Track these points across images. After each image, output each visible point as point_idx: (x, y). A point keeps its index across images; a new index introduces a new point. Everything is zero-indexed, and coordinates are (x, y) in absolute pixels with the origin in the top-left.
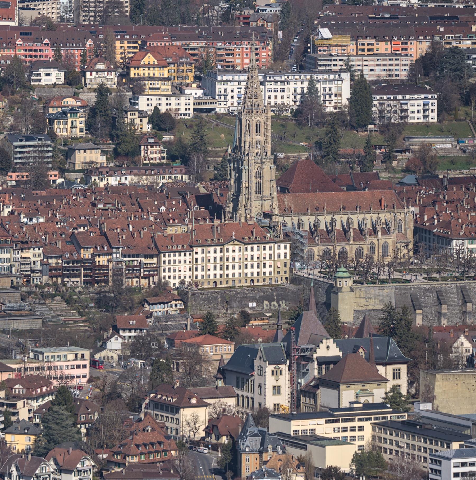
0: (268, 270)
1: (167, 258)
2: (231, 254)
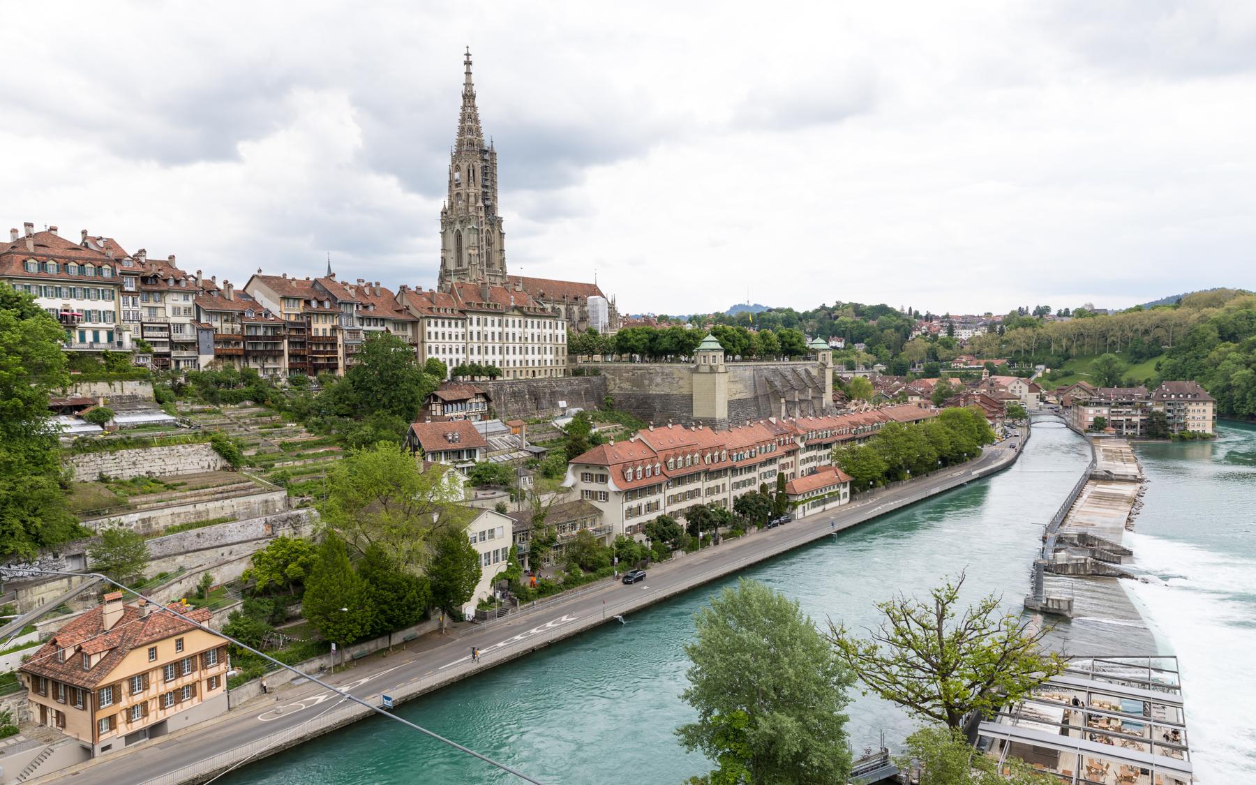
0: (549, 357)
1: (432, 329)
2: (510, 330)
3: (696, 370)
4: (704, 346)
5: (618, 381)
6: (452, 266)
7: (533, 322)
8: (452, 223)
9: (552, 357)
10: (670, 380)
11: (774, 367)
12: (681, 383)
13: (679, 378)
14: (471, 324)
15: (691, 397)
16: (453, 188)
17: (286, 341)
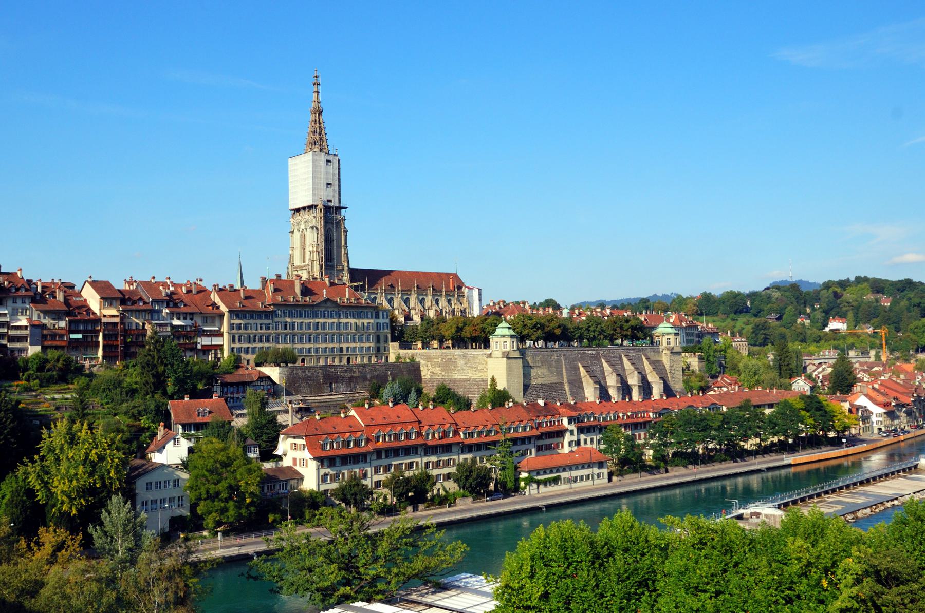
3: (490, 356)
4: (499, 331)
5: (430, 367)
9: (372, 345)
11: (594, 352)
17: (101, 334)
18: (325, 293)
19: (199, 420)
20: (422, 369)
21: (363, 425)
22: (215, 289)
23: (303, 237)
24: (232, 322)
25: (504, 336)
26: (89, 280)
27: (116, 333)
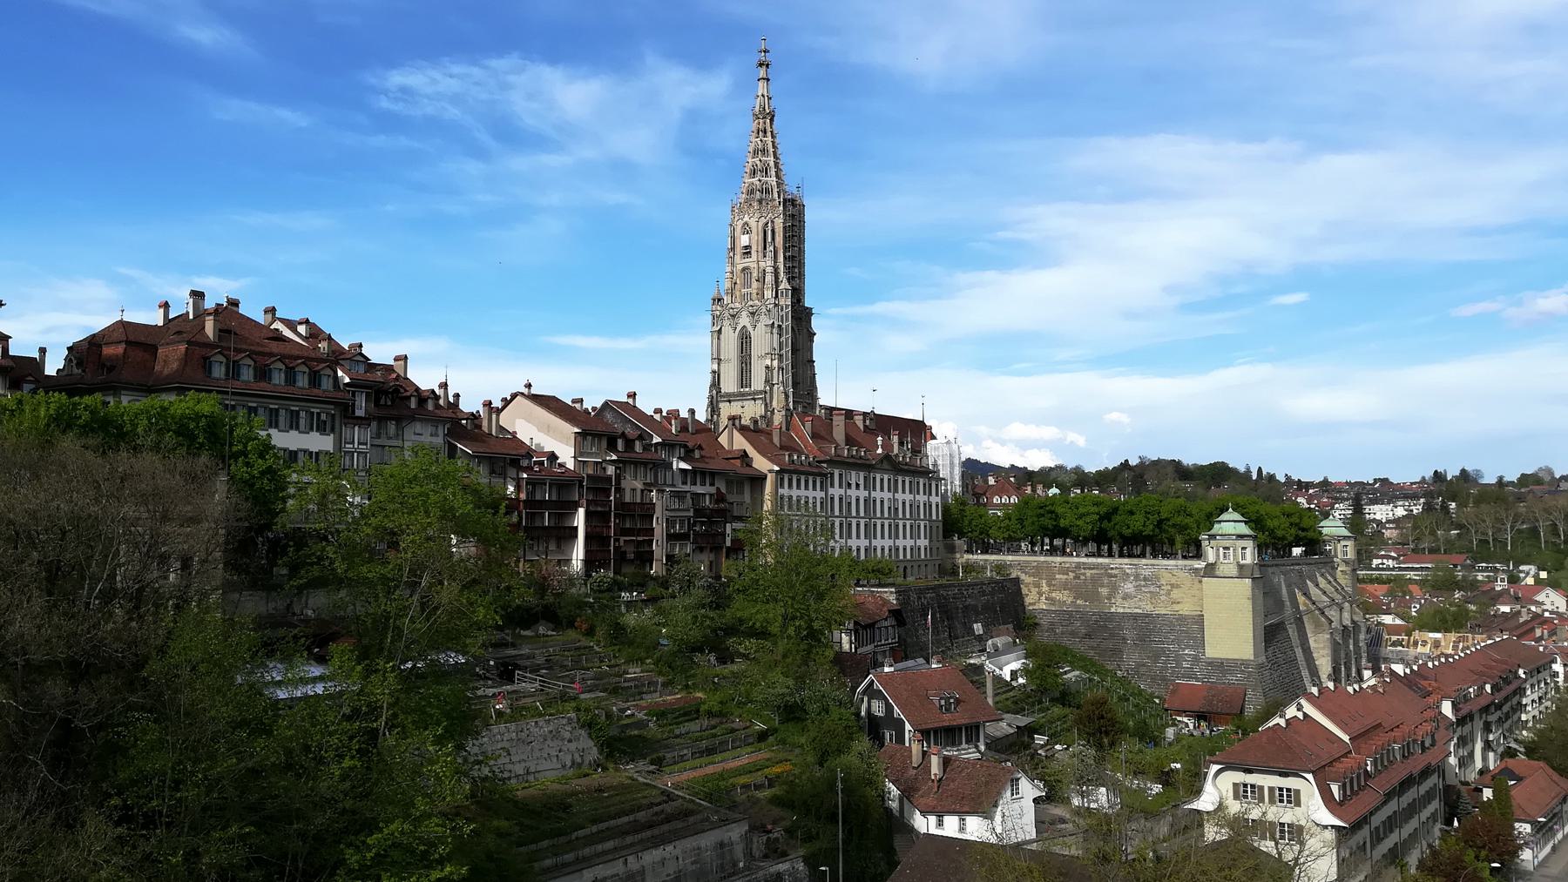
2: (877, 494)
3: (1210, 570)
5: (1045, 588)
6: (729, 385)
7: (904, 482)
8: (733, 316)
9: (926, 542)
10: (1152, 589)
12: (1175, 594)
13: (1172, 586)
14: (832, 485)
15: (1200, 620)
16: (737, 258)
17: (581, 511)
18: (880, 443)
19: (947, 720)
20: (1024, 591)
21: (1346, 738)
22: (734, 425)
23: (745, 340)
24: (785, 491)
25: (1240, 537)
26: (526, 391)
27: (608, 509)
